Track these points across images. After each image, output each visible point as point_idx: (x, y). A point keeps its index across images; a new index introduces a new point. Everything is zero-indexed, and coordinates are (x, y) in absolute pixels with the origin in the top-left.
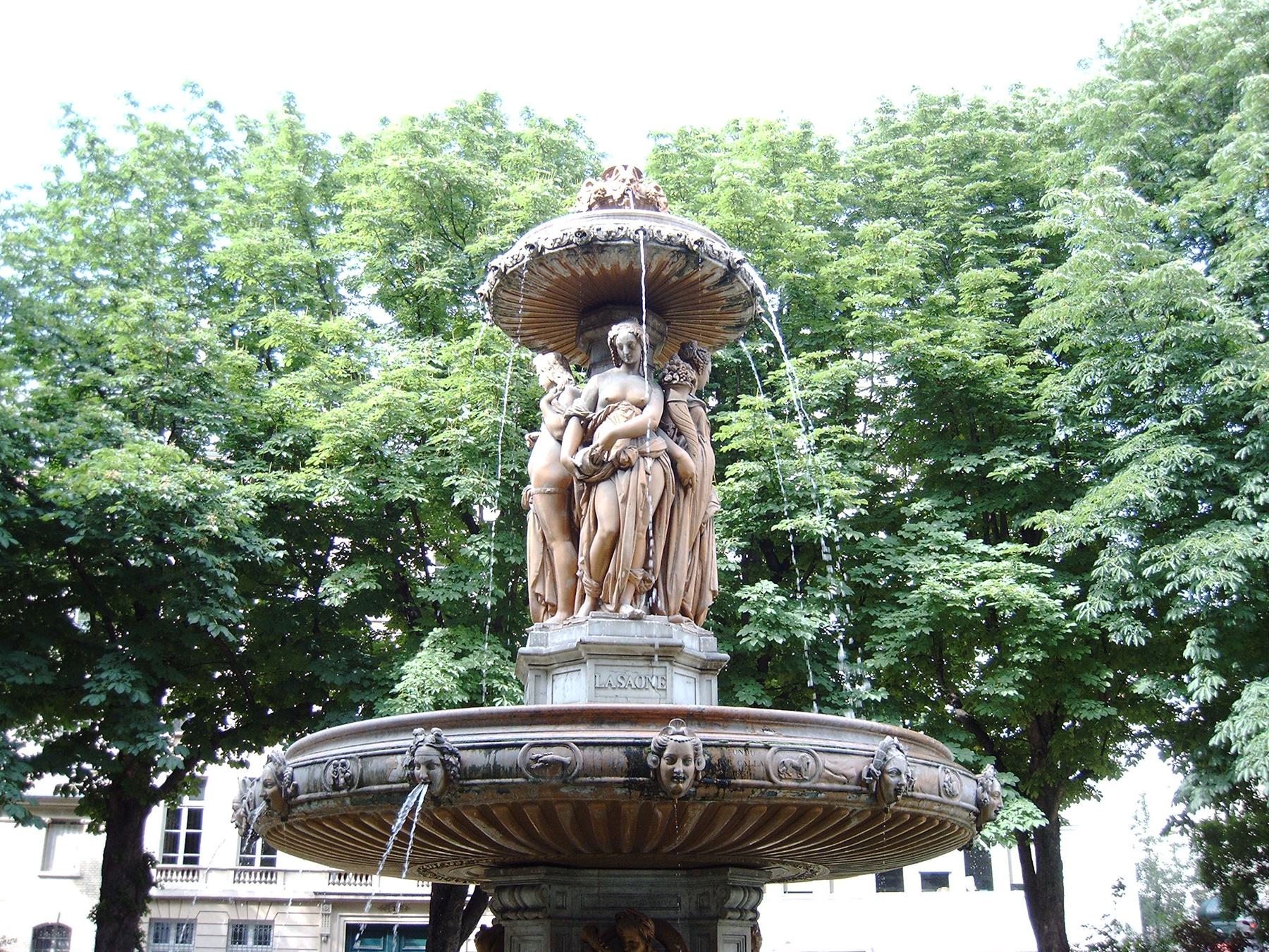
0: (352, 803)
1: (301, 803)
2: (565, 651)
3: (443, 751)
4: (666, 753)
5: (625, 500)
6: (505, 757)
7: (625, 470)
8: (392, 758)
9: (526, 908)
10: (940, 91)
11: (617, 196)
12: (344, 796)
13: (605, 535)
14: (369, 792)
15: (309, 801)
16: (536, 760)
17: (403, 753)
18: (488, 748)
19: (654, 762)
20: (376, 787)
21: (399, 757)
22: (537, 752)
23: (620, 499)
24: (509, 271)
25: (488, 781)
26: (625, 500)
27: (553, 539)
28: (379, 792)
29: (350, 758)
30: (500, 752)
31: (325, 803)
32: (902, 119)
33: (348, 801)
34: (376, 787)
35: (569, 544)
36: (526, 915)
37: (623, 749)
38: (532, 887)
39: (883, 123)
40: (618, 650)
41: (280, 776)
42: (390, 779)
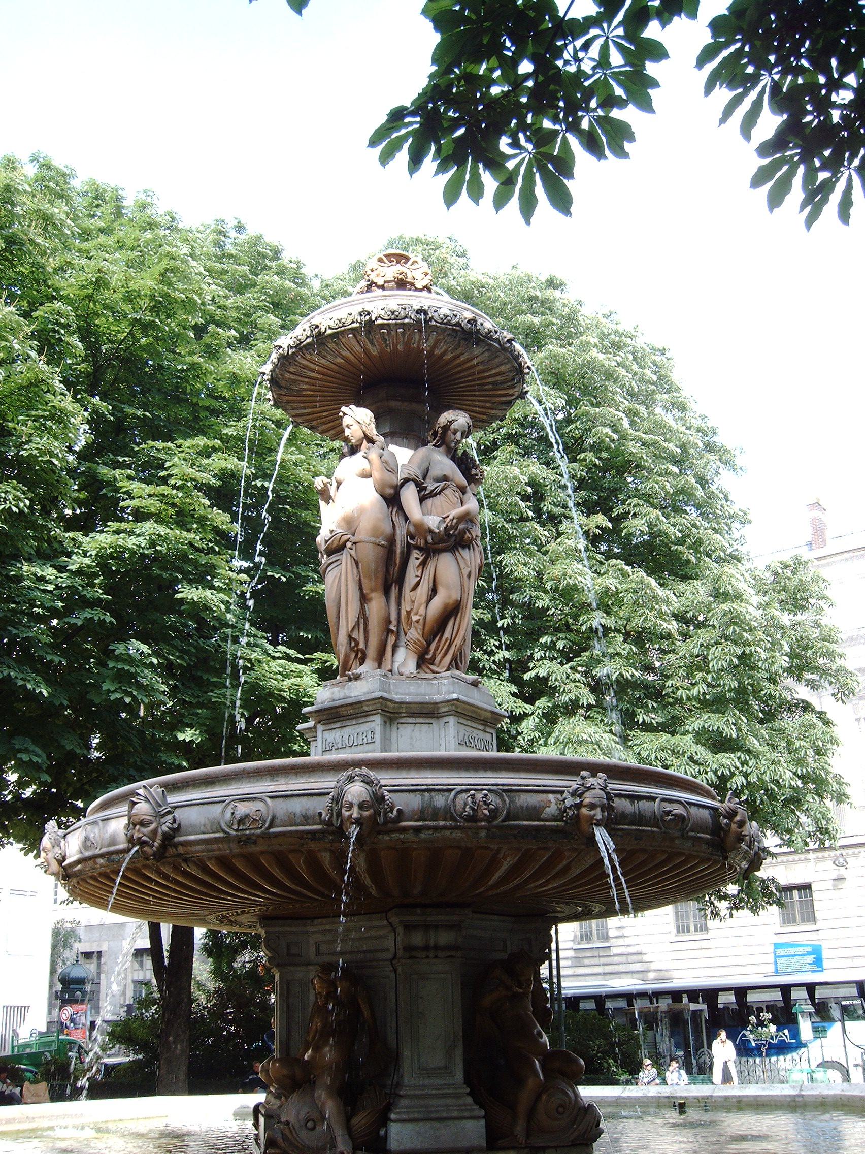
0: (487, 836)
1: (405, 830)
2: (422, 703)
3: (607, 794)
4: (738, 818)
5: (469, 576)
6: (644, 805)
7: (464, 547)
8: (544, 796)
9: (436, 948)
10: (271, 238)
11: (419, 285)
12: (482, 828)
13: (451, 601)
14: (518, 827)
15: (417, 830)
16: (668, 813)
17: (562, 793)
18: (634, 798)
19: (727, 825)
20: (525, 823)
21: (551, 797)
22: (668, 807)
23: (465, 572)
24: (380, 321)
25: (634, 827)
26: (469, 576)
27: (372, 590)
28: (527, 828)
29: (489, 790)
30: (641, 803)
31: (447, 833)
32: (230, 249)
33: (483, 834)
34: (525, 823)
35: (383, 599)
36: (441, 954)
37: (707, 811)
38: (451, 927)
39: (218, 244)
40: (474, 712)
41: (378, 799)
42: (543, 816)
